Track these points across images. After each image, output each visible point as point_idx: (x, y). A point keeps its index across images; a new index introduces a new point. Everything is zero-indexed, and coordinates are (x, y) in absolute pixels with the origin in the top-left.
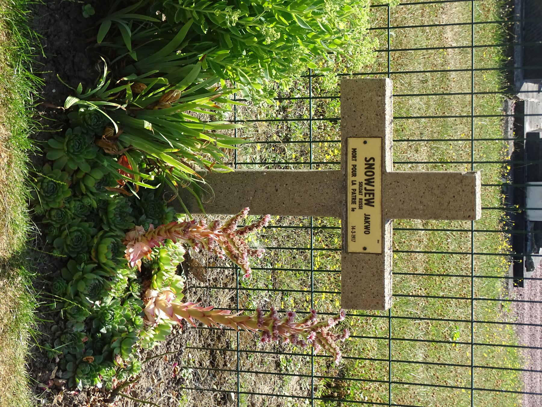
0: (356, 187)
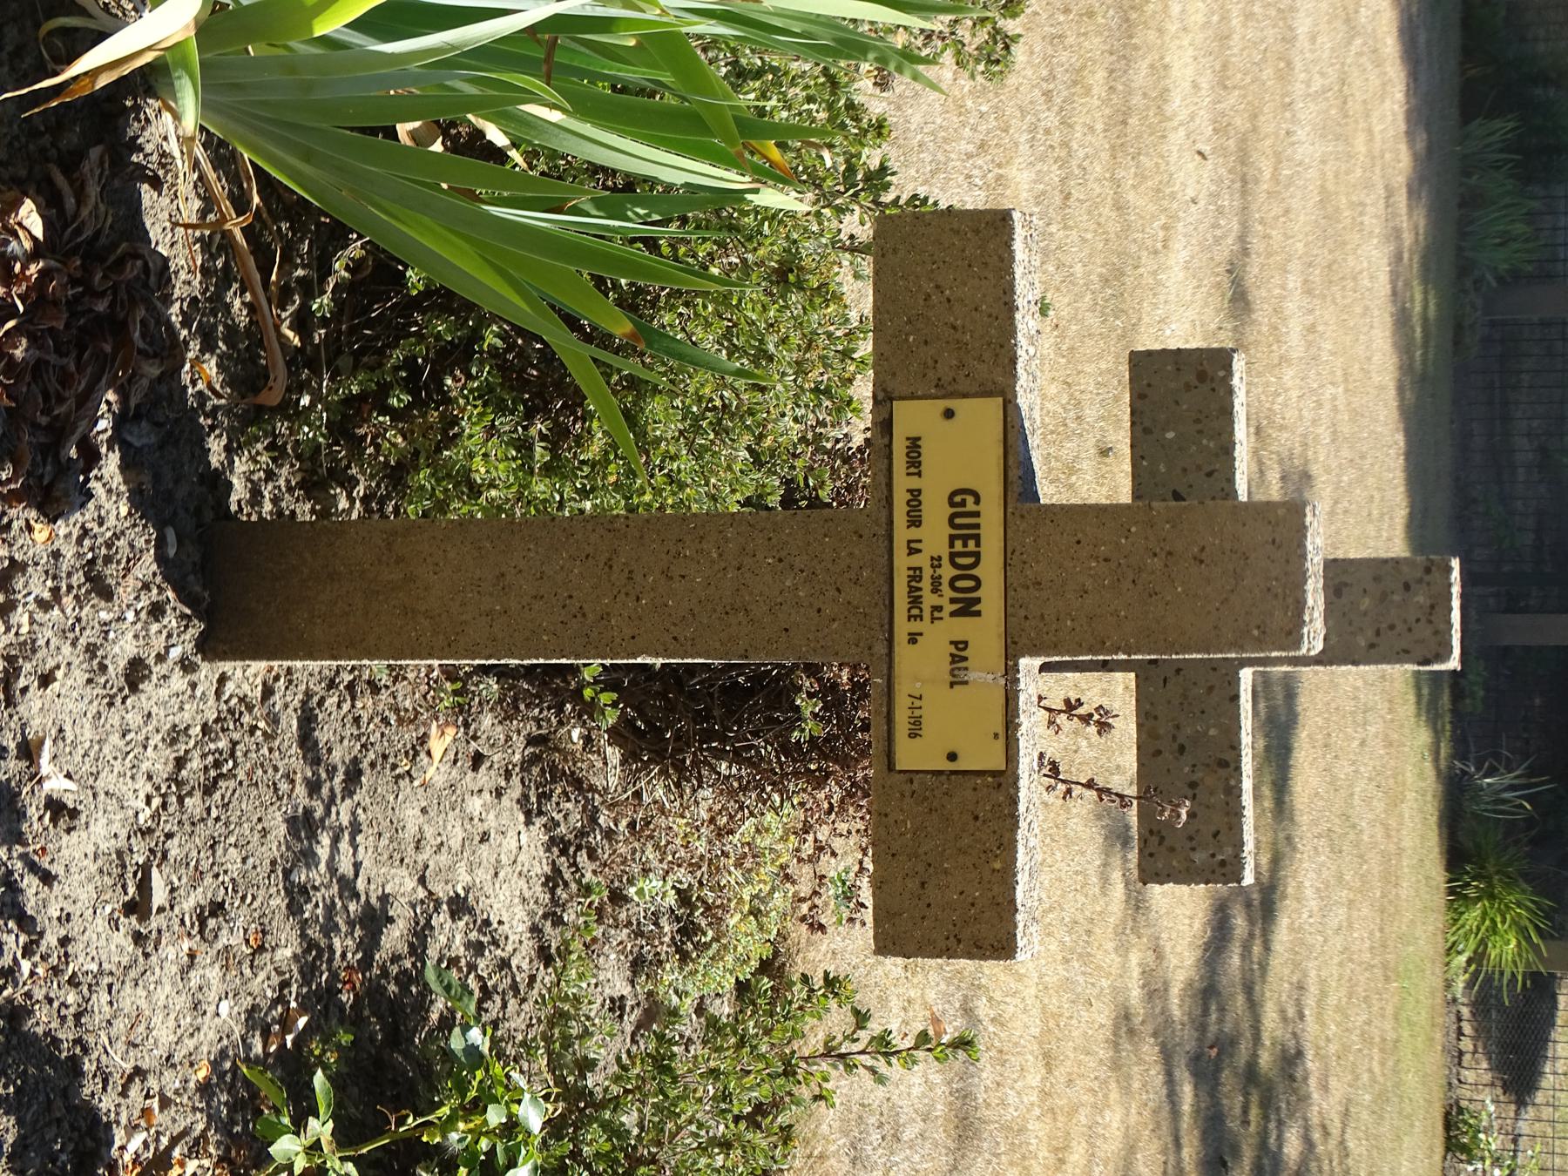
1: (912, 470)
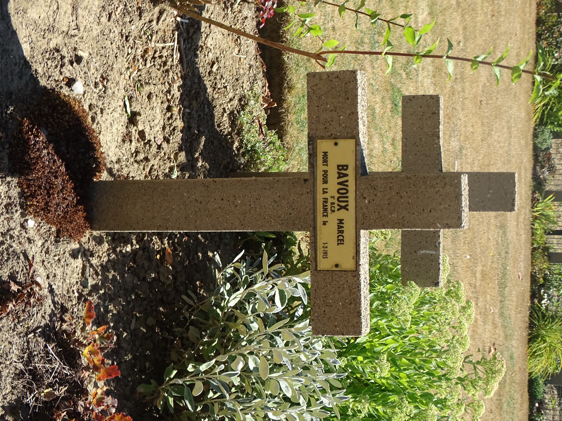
1: (325, 163)
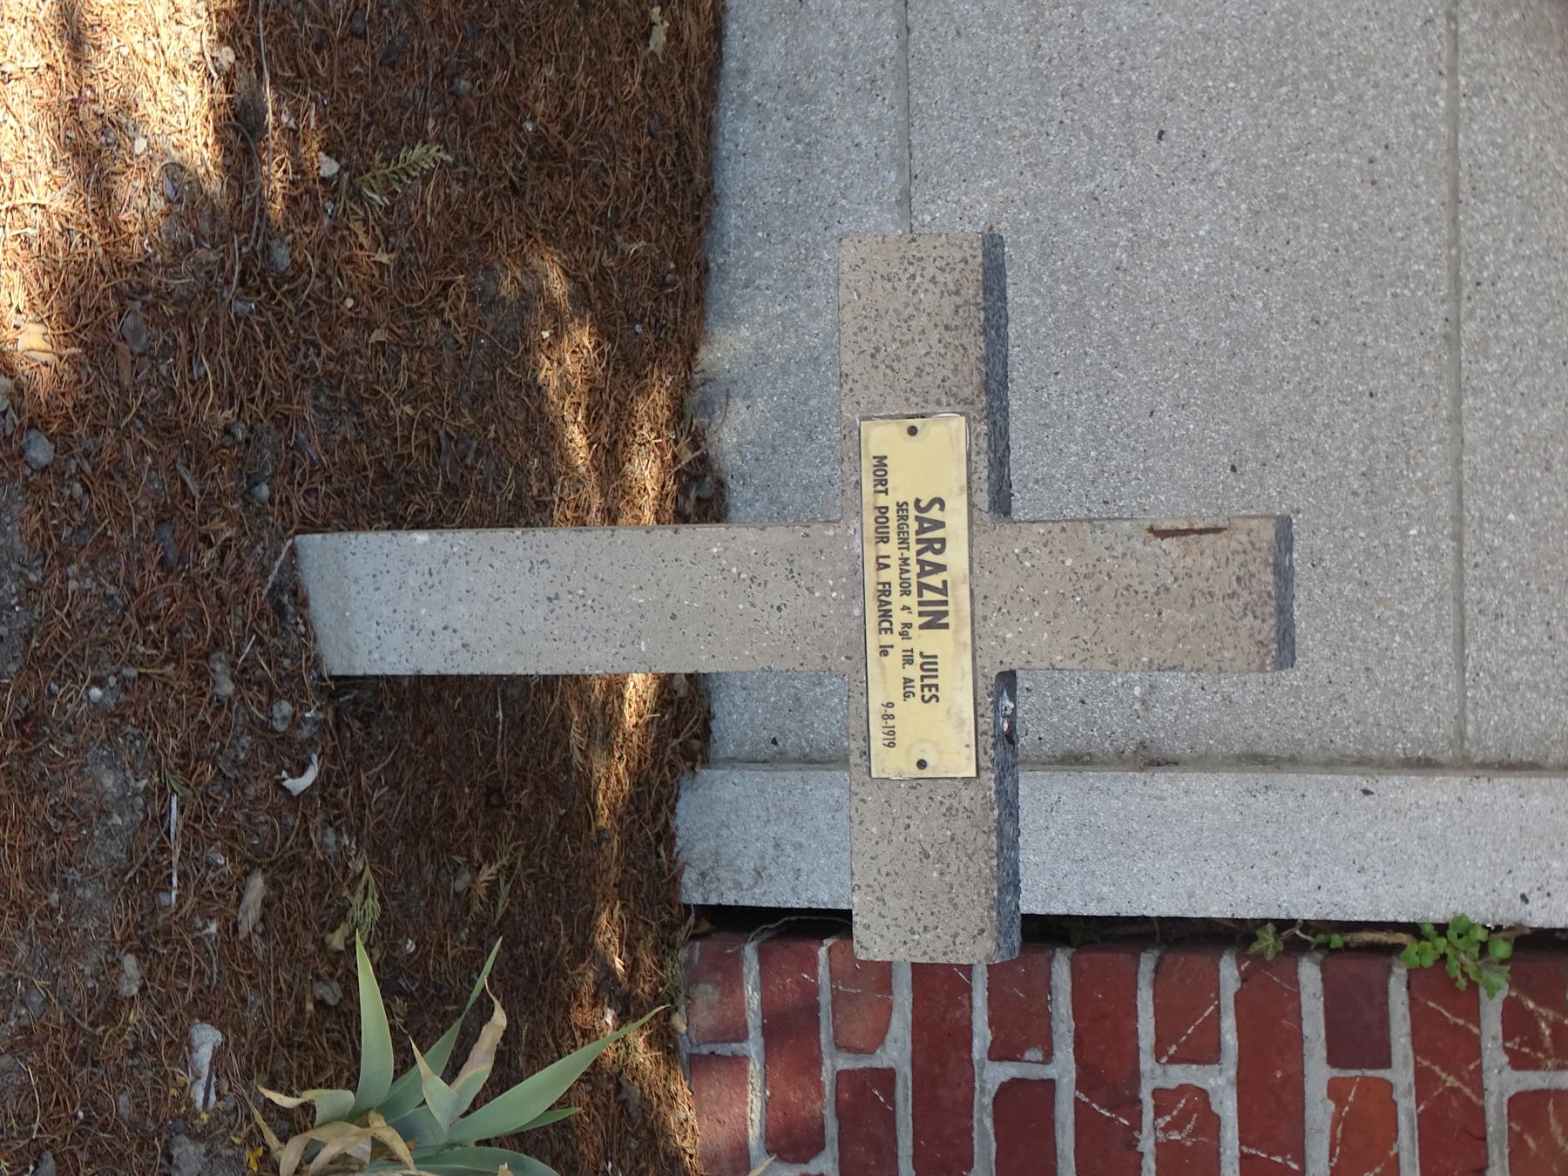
0: (891, 575)
1: (880, 488)
